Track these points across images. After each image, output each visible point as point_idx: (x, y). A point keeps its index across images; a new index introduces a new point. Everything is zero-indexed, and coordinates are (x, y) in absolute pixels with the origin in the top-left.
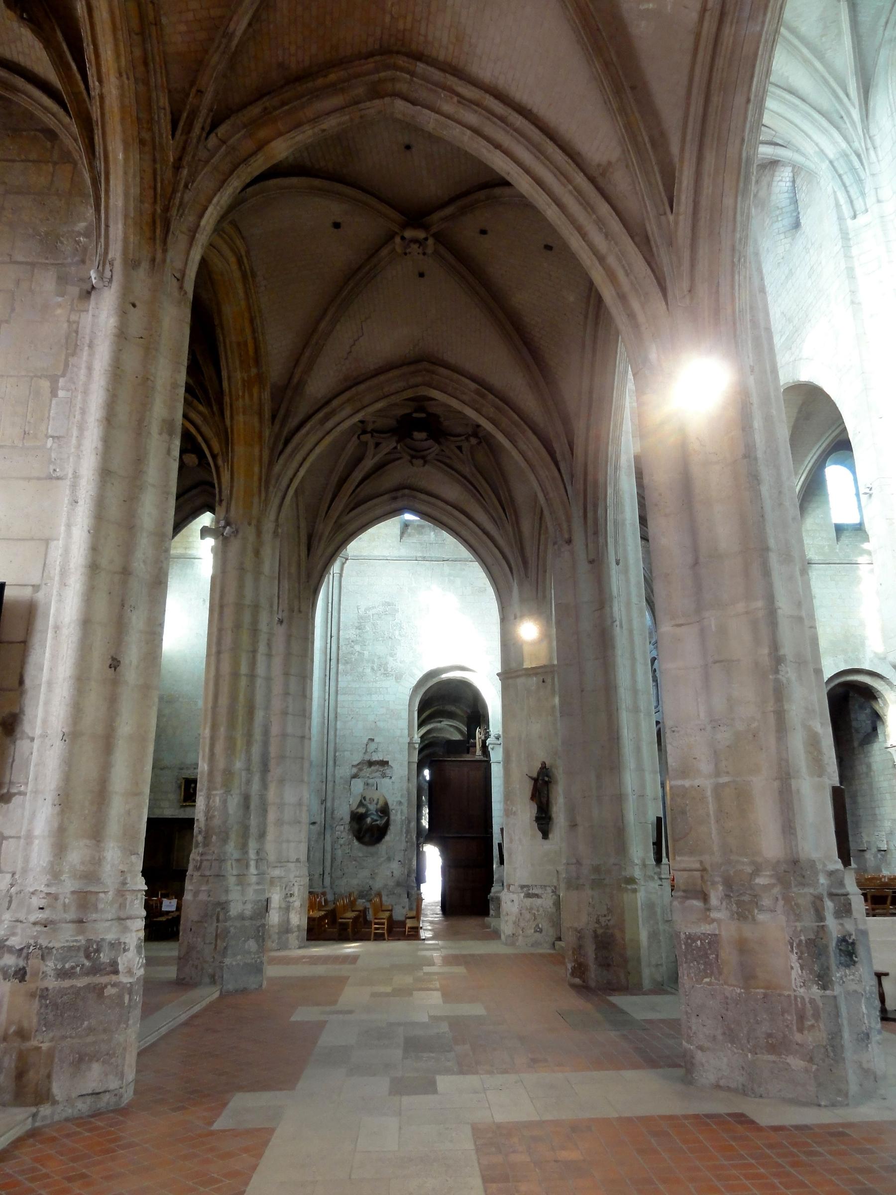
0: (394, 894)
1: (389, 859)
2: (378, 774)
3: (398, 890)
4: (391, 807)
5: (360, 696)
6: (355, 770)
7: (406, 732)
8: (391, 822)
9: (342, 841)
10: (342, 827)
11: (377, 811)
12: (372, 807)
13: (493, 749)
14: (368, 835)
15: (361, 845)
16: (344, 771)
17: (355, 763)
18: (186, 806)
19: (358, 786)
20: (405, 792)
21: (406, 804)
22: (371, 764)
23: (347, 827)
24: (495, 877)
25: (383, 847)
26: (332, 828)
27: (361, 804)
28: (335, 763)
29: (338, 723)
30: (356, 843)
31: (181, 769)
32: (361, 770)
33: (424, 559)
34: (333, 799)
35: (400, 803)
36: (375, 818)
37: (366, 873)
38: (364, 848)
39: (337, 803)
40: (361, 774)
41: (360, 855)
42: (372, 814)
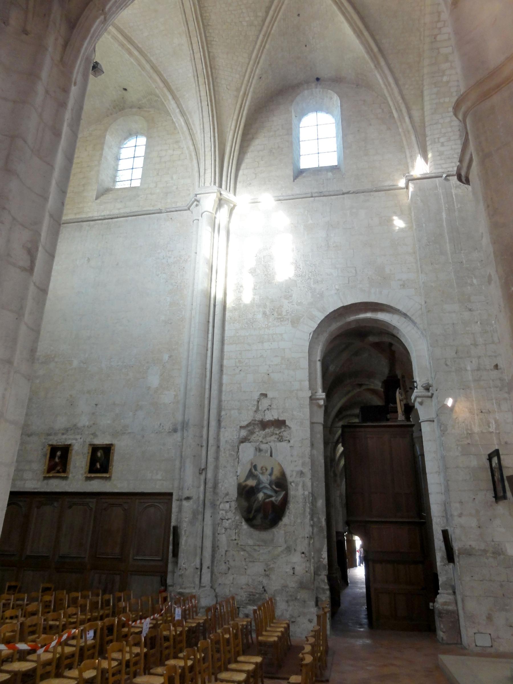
0: (296, 599)
1: (289, 550)
2: (273, 438)
3: (303, 595)
4: (289, 479)
5: (249, 344)
6: (244, 433)
7: (307, 383)
8: (291, 499)
9: (226, 524)
10: (227, 506)
11: (270, 484)
12: (265, 479)
13: (421, 403)
14: (260, 516)
15: (252, 530)
16: (229, 434)
17: (244, 424)
18: (50, 478)
19: (247, 452)
20: (308, 460)
21: (309, 475)
22: (264, 425)
23: (234, 504)
24: (442, 579)
25: (278, 533)
26: (214, 506)
27: (251, 475)
28: (219, 421)
29: (225, 377)
30: (245, 526)
31: (49, 435)
32: (252, 433)
33: (321, 195)
34: (216, 468)
35: (302, 473)
36: (269, 492)
37: (258, 568)
38: (256, 533)
39: (221, 473)
40: (253, 438)
41: (250, 542)
42: (265, 487)
